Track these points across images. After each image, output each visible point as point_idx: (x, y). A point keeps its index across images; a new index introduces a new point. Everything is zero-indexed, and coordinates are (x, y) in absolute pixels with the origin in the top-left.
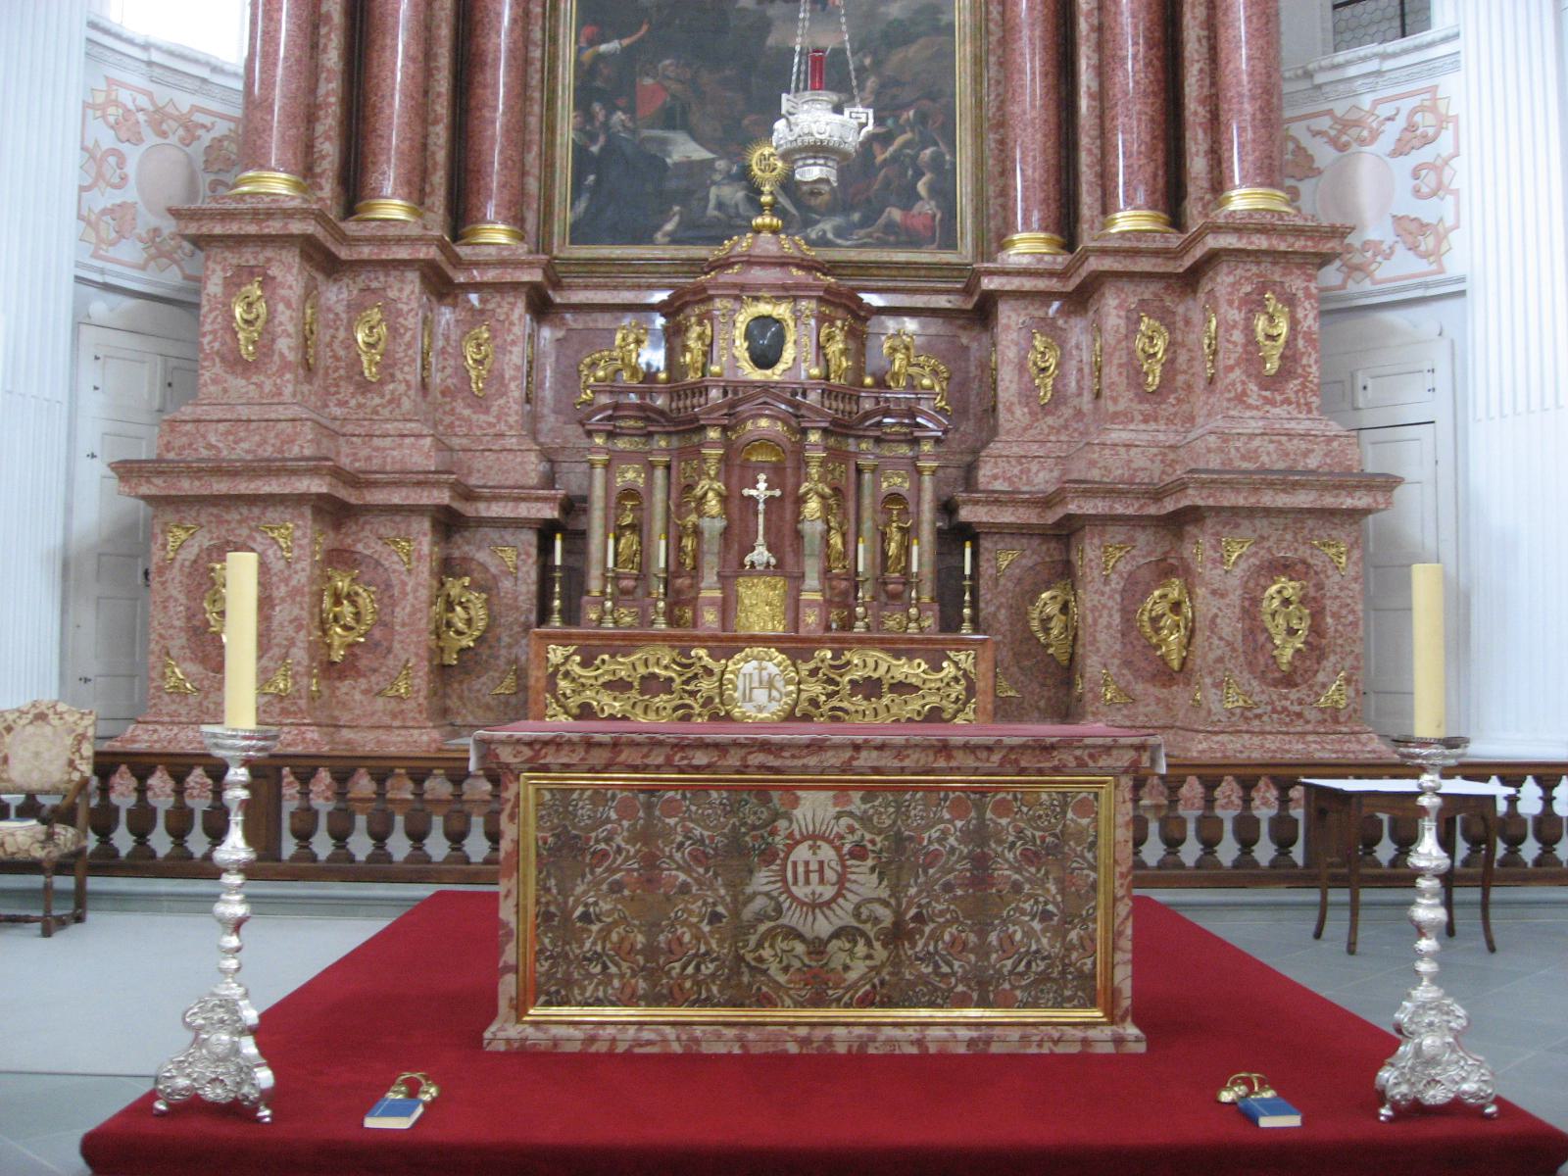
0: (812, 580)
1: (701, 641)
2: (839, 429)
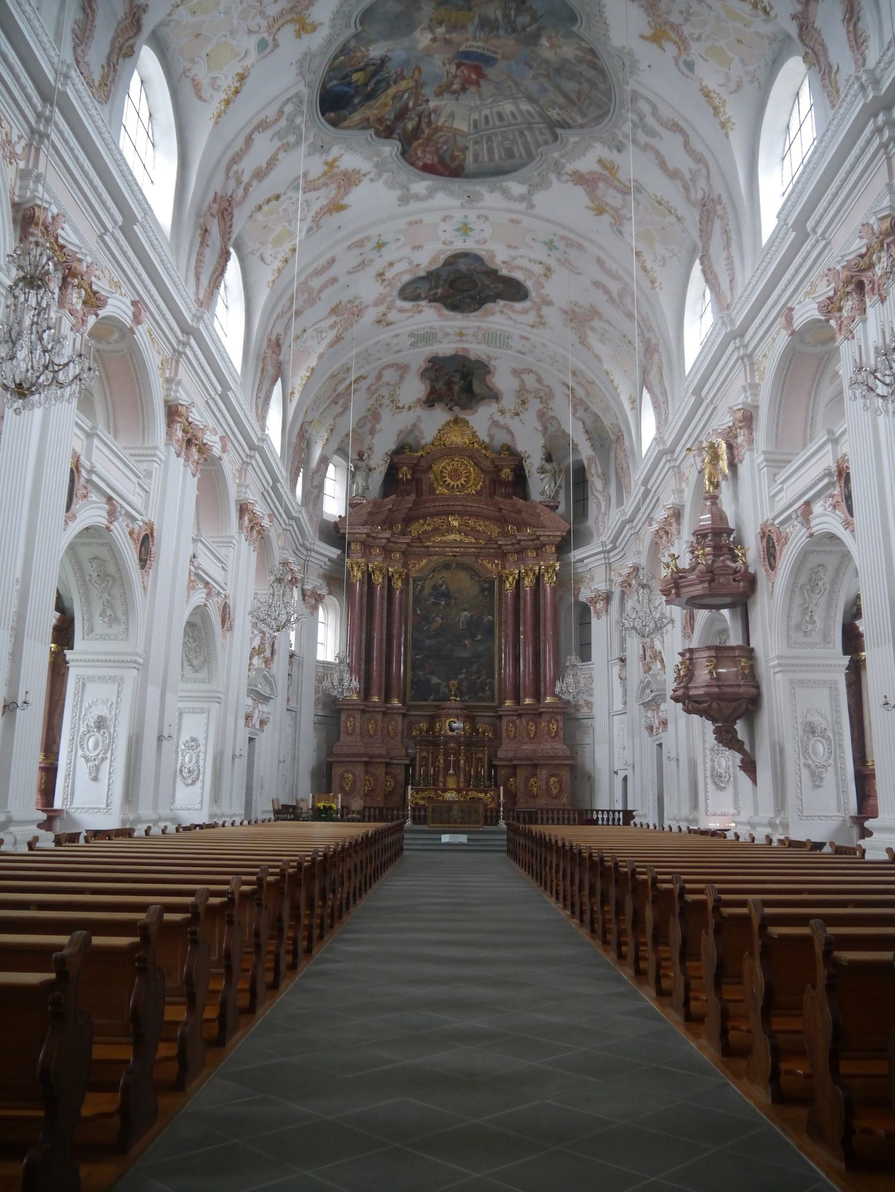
0: (462, 777)
1: (440, 789)
2: (469, 745)
